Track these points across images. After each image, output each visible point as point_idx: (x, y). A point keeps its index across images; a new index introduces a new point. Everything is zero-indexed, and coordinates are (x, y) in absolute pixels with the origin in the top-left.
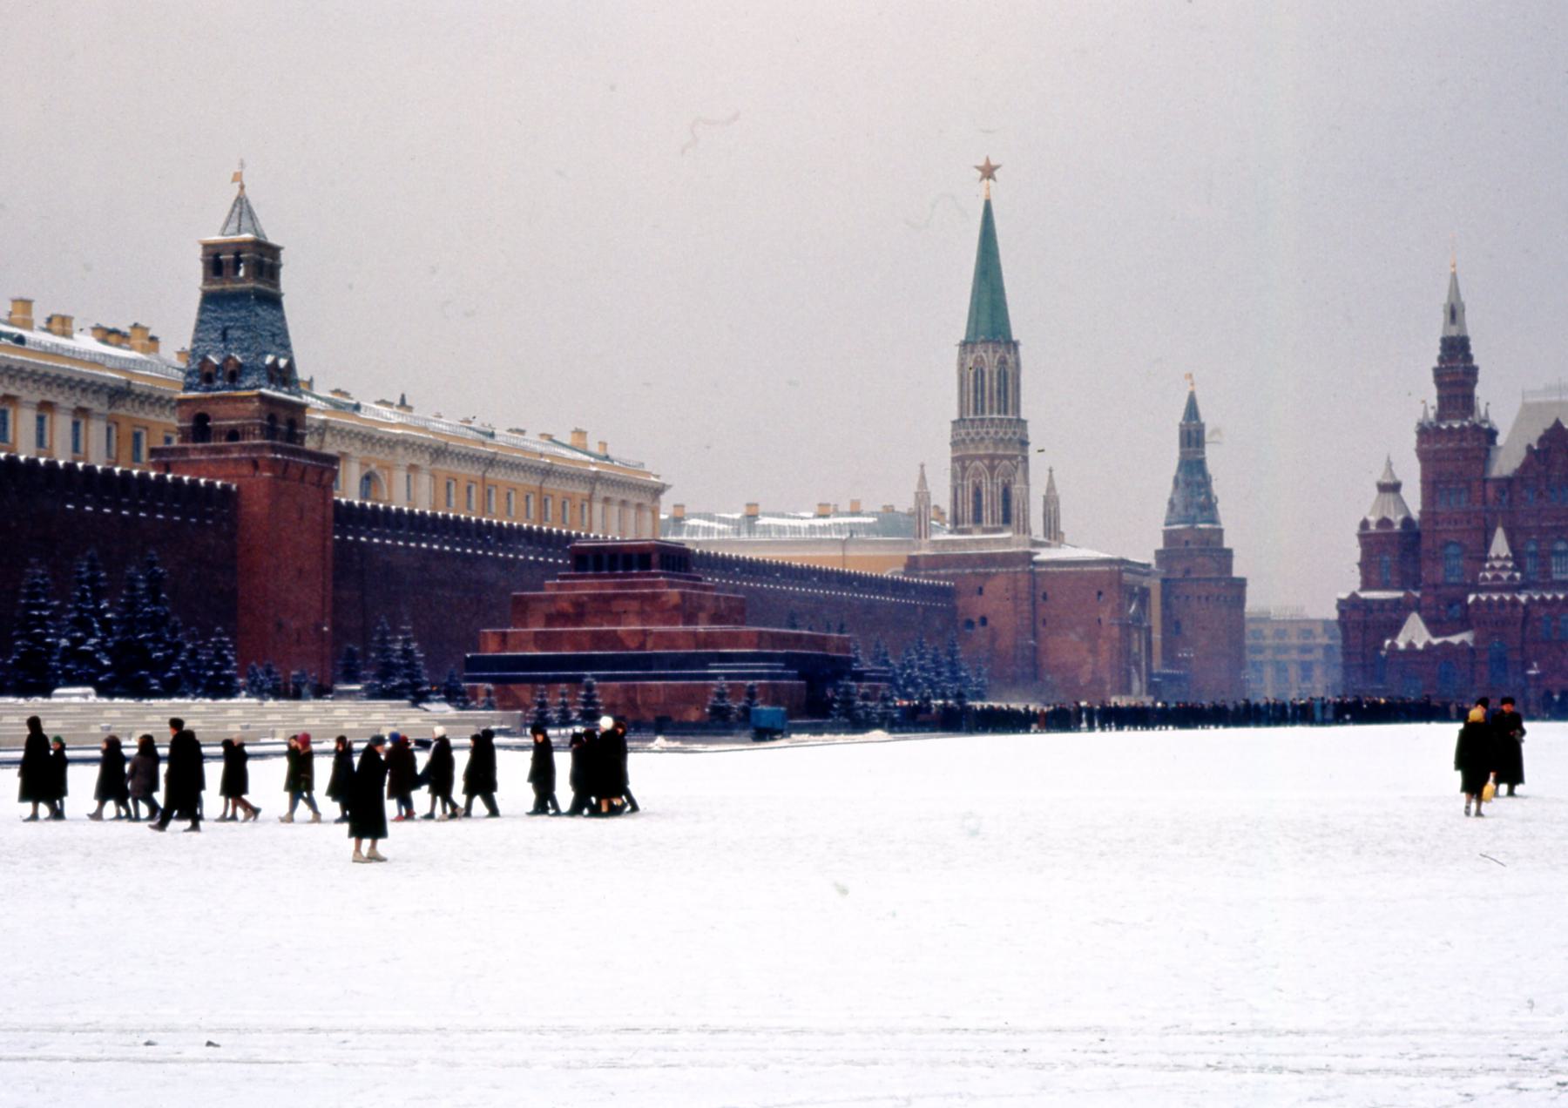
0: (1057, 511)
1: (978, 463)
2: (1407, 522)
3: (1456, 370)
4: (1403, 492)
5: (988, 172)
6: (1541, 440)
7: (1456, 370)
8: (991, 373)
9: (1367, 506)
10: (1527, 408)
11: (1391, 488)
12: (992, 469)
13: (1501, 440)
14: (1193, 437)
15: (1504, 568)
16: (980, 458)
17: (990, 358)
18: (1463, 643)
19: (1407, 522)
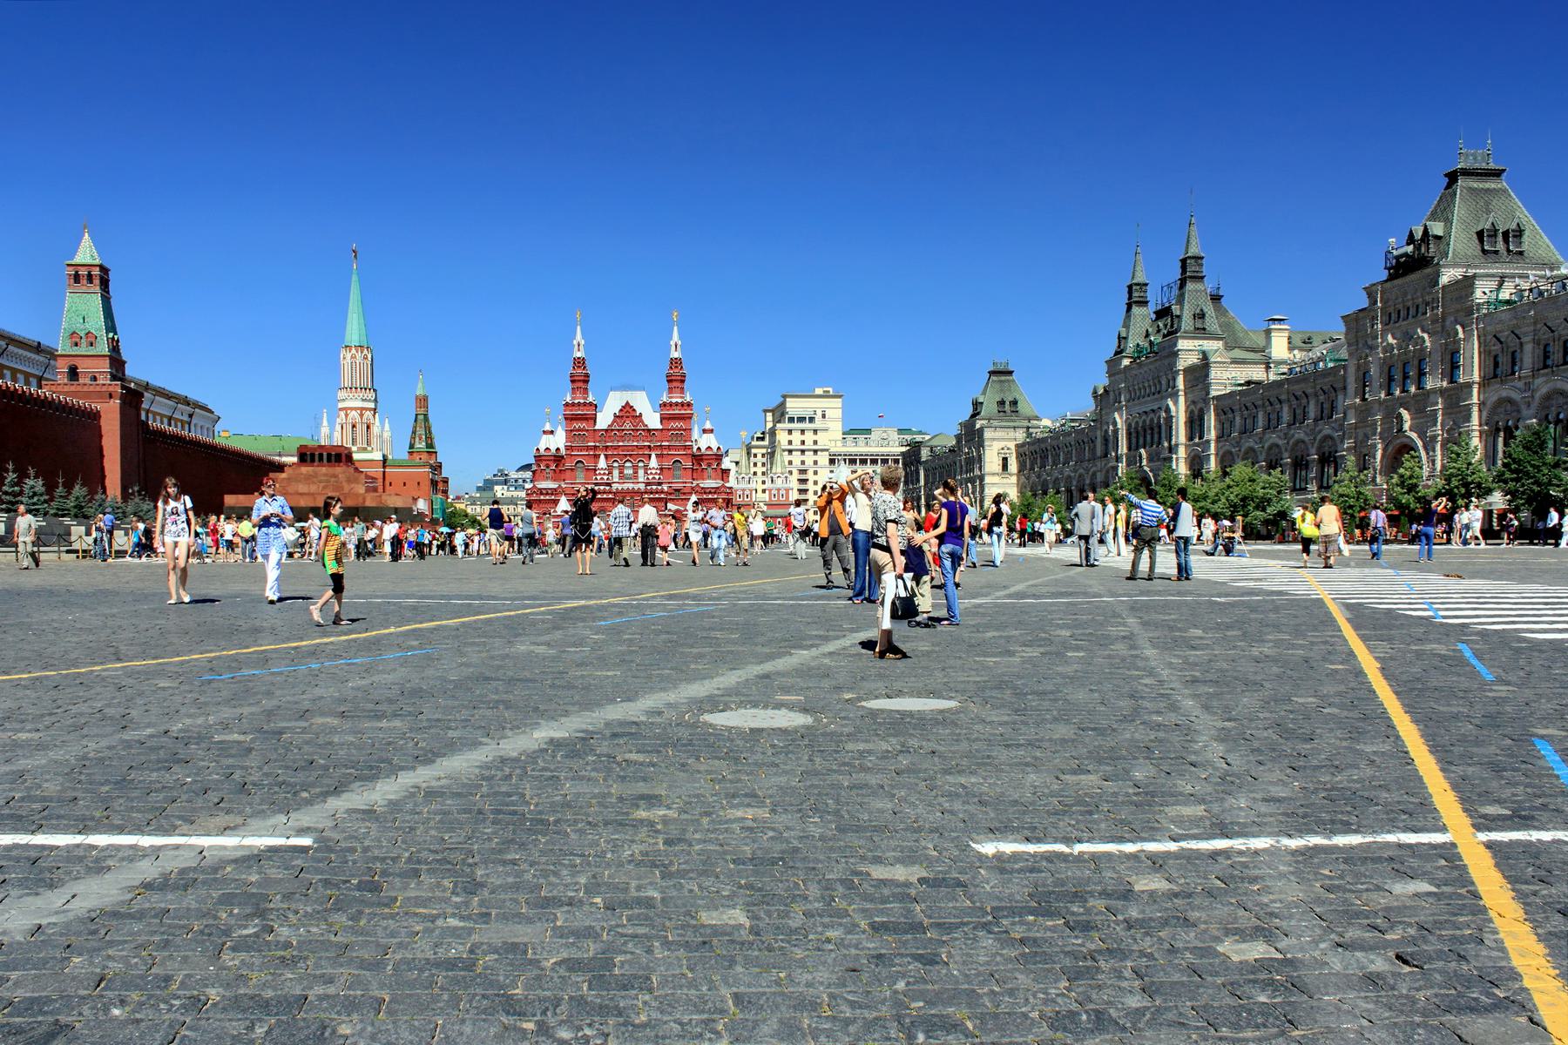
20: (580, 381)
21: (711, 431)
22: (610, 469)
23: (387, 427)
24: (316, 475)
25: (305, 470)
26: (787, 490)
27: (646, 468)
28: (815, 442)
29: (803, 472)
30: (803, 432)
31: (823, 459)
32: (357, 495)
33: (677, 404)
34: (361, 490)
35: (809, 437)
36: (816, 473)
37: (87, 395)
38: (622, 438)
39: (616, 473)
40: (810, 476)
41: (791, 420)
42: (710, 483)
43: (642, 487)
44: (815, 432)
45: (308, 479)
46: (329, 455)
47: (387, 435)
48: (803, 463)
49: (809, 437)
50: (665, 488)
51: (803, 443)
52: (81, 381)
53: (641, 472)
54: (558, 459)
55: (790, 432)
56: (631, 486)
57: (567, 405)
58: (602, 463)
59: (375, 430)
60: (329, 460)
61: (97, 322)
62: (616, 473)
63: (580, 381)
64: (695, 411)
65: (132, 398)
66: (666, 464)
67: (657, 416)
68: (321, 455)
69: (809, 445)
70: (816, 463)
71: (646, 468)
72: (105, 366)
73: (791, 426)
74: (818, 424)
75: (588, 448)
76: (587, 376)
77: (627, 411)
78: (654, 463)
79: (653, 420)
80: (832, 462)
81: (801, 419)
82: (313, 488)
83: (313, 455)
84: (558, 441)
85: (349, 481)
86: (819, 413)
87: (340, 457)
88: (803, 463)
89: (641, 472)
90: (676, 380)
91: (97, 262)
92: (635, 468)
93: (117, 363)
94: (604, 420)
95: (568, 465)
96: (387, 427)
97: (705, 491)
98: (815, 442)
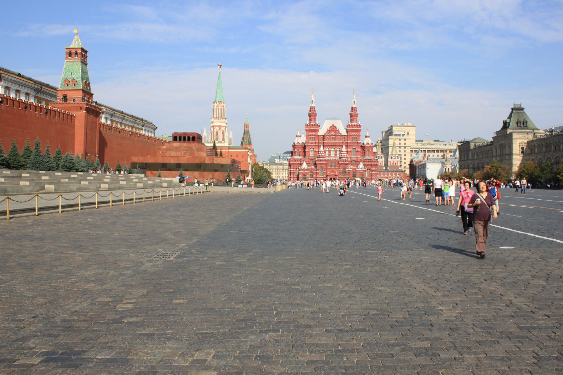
12: (220, 129)
14: (246, 126)
16: (218, 126)
20: (312, 115)
21: (369, 137)
23: (231, 133)
24: (180, 147)
25: (176, 144)
28: (405, 144)
29: (400, 155)
30: (400, 140)
31: (408, 150)
32: (201, 157)
33: (355, 125)
34: (204, 155)
35: (402, 142)
36: (405, 155)
37: (70, 109)
39: (327, 152)
40: (403, 157)
41: (395, 135)
42: (367, 158)
44: (405, 140)
45: (177, 149)
46: (189, 138)
47: (231, 136)
48: (400, 151)
49: (402, 142)
51: (400, 144)
52: (68, 102)
56: (334, 158)
57: (307, 125)
58: (322, 149)
59: (226, 134)
60: (189, 140)
61: (77, 76)
62: (327, 152)
63: (312, 115)
64: (362, 128)
65: (94, 111)
67: (345, 131)
68: (185, 138)
69: (402, 144)
70: (405, 151)
72: (80, 95)
74: (406, 137)
75: (315, 143)
76: (316, 114)
77: (333, 128)
78: (344, 149)
79: (343, 132)
80: (412, 151)
81: (399, 135)
82: (179, 154)
83: (180, 138)
84: (303, 140)
85: (198, 150)
86: (406, 133)
87: (194, 138)
88: (400, 151)
89: (338, 153)
90: (353, 115)
91: (81, 47)
93: (87, 93)
94: (322, 132)
95: (307, 150)
96: (231, 133)
97: (365, 161)
98: (405, 144)
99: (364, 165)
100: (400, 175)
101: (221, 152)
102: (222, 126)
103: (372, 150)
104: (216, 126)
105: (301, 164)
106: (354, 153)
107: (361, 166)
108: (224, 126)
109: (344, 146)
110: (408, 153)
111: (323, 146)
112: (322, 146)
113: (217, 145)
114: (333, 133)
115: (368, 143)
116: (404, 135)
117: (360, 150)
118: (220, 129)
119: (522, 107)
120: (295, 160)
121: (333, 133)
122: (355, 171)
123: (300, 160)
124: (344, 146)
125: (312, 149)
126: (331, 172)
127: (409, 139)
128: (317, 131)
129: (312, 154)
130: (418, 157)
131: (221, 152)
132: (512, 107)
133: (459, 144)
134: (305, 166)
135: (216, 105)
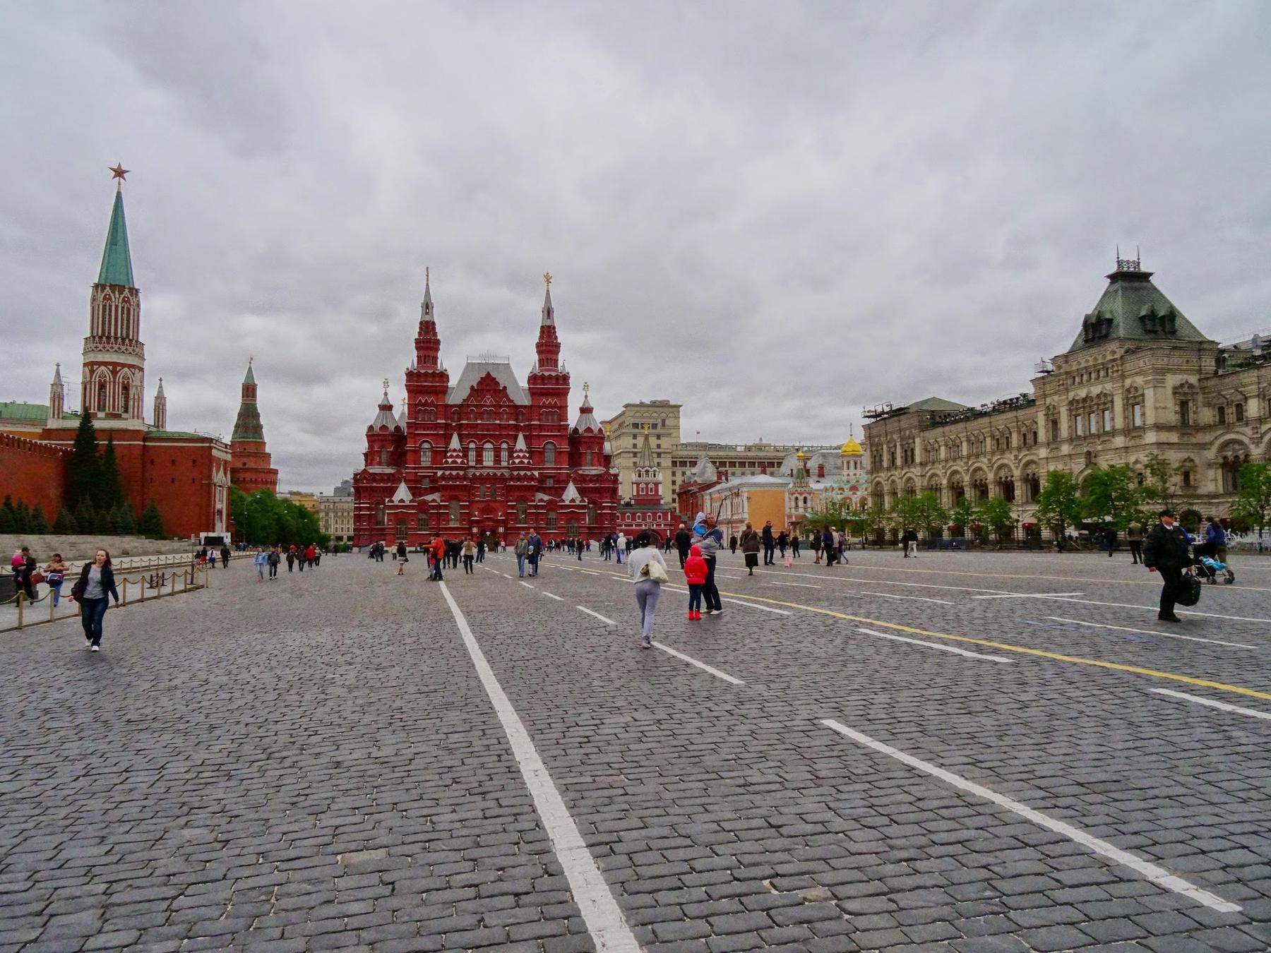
0: (164, 405)
1: (103, 368)
2: (397, 428)
3: (428, 342)
4: (394, 411)
5: (119, 173)
6: (479, 383)
7: (428, 342)
8: (117, 307)
9: (372, 416)
10: (470, 366)
11: (386, 408)
12: (114, 373)
13: (453, 382)
14: (249, 391)
15: (458, 456)
16: (106, 364)
17: (116, 299)
18: (434, 501)
19: (397, 428)
22: (465, 451)
26: (656, 484)
27: (511, 451)
28: (659, 446)
33: (550, 377)
38: (480, 415)
39: (472, 455)
43: (507, 473)
44: (658, 437)
50: (536, 473)
53: (504, 455)
54: (398, 437)
55: (635, 437)
56: (491, 472)
58: (455, 443)
62: (472, 455)
66: (535, 446)
71: (511, 451)
73: (636, 431)
74: (659, 430)
75: (437, 427)
78: (521, 444)
80: (674, 463)
89: (504, 455)
92: (497, 451)
95: (410, 446)
98: (659, 446)
99: (581, 491)
100: (666, 519)
101: (110, 446)
102: (123, 365)
103: (601, 448)
104: (100, 364)
105: (392, 491)
106: (550, 455)
107: (571, 493)
108: (130, 366)
109: (521, 436)
110: (666, 468)
111: (461, 437)
112: (455, 438)
113: (97, 424)
114: (489, 400)
115: (589, 430)
116: (655, 426)
117: (566, 447)
118: (114, 373)
119: (1144, 268)
120: (374, 477)
121: (489, 400)
122: (552, 506)
123: (390, 478)
124: (521, 436)
125: (426, 446)
126: (482, 511)
127: (669, 435)
128: (444, 390)
129: (426, 460)
130: (702, 474)
131: (110, 446)
132: (1113, 269)
133: (868, 421)
134: (403, 493)
135: (101, 297)
